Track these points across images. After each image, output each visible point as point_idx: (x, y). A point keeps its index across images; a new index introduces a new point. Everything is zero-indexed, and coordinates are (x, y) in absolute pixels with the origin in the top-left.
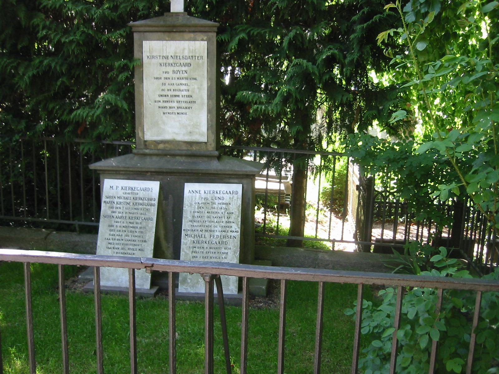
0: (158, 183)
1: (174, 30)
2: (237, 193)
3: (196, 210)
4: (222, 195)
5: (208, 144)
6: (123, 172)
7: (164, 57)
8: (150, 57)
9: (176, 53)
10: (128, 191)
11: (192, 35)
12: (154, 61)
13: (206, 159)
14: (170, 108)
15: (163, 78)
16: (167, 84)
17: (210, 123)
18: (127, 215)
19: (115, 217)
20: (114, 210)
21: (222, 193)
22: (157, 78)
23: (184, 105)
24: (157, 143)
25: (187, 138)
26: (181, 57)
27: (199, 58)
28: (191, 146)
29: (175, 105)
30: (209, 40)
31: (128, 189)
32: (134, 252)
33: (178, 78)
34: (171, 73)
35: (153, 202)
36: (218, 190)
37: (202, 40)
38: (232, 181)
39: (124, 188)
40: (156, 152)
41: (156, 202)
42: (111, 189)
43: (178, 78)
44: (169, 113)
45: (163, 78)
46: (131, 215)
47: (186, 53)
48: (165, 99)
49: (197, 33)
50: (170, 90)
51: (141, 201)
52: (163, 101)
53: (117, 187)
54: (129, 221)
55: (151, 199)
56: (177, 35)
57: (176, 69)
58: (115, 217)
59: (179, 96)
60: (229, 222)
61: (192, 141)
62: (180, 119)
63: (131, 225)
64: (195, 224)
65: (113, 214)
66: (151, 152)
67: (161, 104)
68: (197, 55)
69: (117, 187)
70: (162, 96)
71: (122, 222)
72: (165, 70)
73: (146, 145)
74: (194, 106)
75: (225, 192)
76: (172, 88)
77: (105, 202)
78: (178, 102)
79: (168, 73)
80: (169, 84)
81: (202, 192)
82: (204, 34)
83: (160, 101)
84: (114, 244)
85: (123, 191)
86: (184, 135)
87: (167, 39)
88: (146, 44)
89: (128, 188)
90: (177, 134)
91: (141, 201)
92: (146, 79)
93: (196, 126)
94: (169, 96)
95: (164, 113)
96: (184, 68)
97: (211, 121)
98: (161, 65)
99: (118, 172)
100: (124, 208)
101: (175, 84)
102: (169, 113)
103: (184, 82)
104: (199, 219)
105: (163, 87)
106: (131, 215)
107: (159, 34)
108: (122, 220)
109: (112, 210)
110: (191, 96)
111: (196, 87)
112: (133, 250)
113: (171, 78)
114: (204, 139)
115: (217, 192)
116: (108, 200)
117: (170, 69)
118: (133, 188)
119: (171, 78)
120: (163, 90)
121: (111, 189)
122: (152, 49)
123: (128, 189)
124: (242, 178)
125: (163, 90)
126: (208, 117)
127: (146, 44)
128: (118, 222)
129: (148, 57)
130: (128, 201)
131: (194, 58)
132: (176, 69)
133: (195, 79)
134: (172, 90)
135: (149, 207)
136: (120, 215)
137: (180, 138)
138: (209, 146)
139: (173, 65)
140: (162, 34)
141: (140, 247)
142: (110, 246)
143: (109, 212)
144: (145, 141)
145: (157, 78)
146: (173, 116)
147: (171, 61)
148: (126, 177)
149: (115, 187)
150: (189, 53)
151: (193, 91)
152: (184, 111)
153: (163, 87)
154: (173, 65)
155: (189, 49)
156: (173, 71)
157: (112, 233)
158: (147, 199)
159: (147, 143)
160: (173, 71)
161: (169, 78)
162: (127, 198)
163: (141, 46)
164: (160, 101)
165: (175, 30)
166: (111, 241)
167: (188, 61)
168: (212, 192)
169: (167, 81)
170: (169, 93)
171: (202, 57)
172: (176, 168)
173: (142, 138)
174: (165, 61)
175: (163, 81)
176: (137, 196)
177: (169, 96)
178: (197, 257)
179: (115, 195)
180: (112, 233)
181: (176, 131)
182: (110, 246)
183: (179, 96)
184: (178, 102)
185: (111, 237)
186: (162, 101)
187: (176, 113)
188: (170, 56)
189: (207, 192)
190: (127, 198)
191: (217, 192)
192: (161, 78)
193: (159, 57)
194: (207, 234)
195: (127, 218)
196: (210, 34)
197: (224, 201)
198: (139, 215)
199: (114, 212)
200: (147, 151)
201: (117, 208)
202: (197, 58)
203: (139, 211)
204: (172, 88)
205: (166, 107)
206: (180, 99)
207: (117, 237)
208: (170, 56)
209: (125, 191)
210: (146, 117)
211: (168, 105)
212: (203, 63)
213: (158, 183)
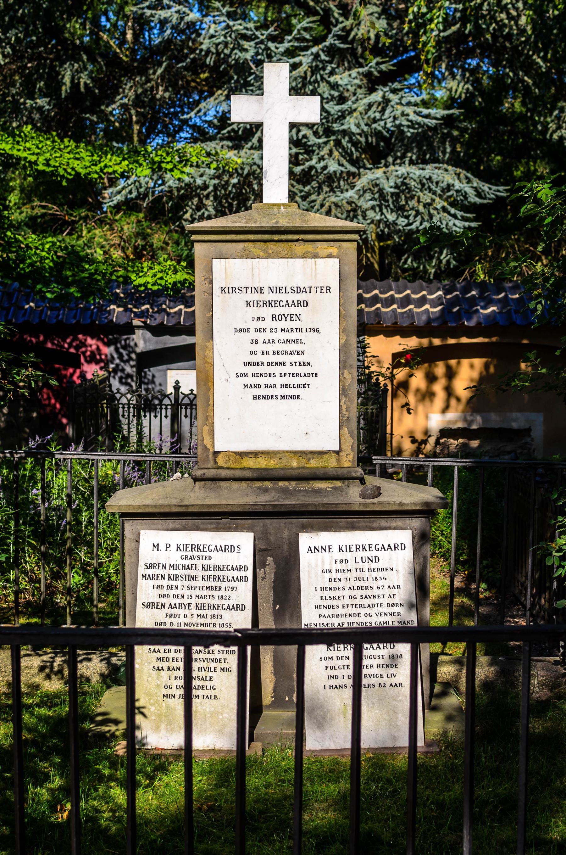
2: (403, 547)
4: (374, 553)
5: (341, 454)
7: (254, 290)
8: (226, 290)
10: (189, 554)
14: (266, 386)
15: (252, 330)
16: (261, 341)
18: (194, 601)
19: (167, 606)
20: (165, 591)
21: (373, 548)
22: (240, 330)
26: (288, 290)
28: (309, 460)
32: (210, 674)
33: (283, 330)
34: (269, 318)
35: (243, 574)
36: (367, 543)
39: (181, 547)
40: (238, 474)
41: (249, 574)
42: (156, 549)
43: (283, 330)
44: (264, 397)
45: (252, 330)
46: (201, 601)
50: (267, 353)
51: (217, 573)
52: (253, 375)
54: (196, 612)
55: (239, 569)
57: (278, 311)
58: (167, 606)
59: (284, 363)
60: (393, 605)
65: (163, 600)
67: (250, 380)
69: (167, 546)
70: (250, 364)
71: (182, 616)
75: (380, 547)
76: (270, 348)
77: (144, 576)
79: (263, 319)
80: (264, 342)
81: (335, 549)
83: (246, 375)
91: (217, 573)
94: (265, 364)
95: (255, 398)
98: (248, 304)
100: (186, 588)
101: (276, 341)
102: (264, 397)
105: (254, 347)
106: (201, 601)
108: (182, 612)
109: (160, 591)
110: (309, 364)
112: (209, 669)
113: (268, 330)
115: (364, 548)
116: (150, 572)
117: (267, 312)
118: (201, 548)
119: (268, 330)
120: (252, 353)
121: (156, 549)
125: (252, 353)
126: (342, 403)
128: (175, 616)
129: (223, 290)
130: (193, 573)
132: (278, 311)
133: (317, 331)
134: (271, 353)
136: (177, 601)
139: (273, 303)
141: (223, 665)
142: (160, 664)
144: (216, 454)
145: (240, 330)
147: (268, 297)
149: (162, 547)
153: (254, 347)
154: (273, 303)
156: (274, 317)
158: (230, 568)
160: (274, 317)
161: (265, 330)
162: (189, 568)
164: (246, 375)
168: (354, 548)
169: (261, 336)
170: (265, 359)
171: (329, 289)
172: (281, 504)
173: (209, 446)
174: (256, 297)
175: (253, 335)
177: (265, 364)
178: (336, 677)
179: (162, 562)
182: (160, 664)
183: (284, 363)
186: (250, 375)
187: (279, 397)
190: (189, 568)
191: (364, 548)
192: (248, 330)
193: (244, 290)
195: (193, 606)
197: (380, 565)
198: (216, 601)
199: (164, 596)
202: (319, 290)
203: (216, 593)
204: (270, 348)
205: (259, 386)
209: (185, 553)
211: (262, 381)
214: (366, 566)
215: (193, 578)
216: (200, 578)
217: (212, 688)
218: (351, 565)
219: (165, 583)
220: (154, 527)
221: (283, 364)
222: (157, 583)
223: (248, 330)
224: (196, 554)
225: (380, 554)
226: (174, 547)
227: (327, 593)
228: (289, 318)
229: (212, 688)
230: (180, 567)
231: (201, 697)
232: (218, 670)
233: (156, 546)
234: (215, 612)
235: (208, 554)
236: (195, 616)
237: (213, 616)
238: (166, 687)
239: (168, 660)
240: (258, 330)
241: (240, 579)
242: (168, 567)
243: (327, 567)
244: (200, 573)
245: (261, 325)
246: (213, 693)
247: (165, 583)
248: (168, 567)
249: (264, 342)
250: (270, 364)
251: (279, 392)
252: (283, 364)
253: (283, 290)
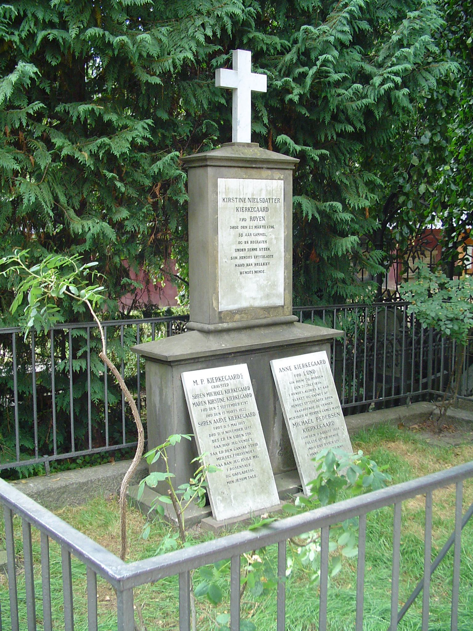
0: (246, 364)
1: (248, 166)
3: (294, 391)
5: (285, 307)
6: (203, 359)
9: (253, 194)
10: (216, 384)
11: (269, 172)
12: (231, 205)
13: (285, 327)
17: (287, 280)
19: (213, 422)
20: (209, 412)
22: (233, 228)
23: (261, 261)
24: (232, 313)
25: (265, 303)
26: (259, 200)
27: (276, 201)
29: (252, 261)
30: (285, 180)
31: (215, 381)
35: (248, 392)
37: (279, 179)
38: (314, 349)
39: (210, 380)
41: (251, 391)
44: (246, 273)
45: (240, 228)
46: (232, 414)
47: (264, 196)
48: (242, 254)
49: (274, 170)
51: (235, 394)
53: (202, 381)
56: (254, 172)
57: (254, 214)
58: (213, 422)
61: (270, 305)
62: (258, 279)
63: (235, 428)
64: (298, 408)
66: (231, 325)
68: (274, 198)
69: (202, 381)
70: (238, 250)
72: (242, 217)
73: (220, 318)
74: (272, 261)
78: (256, 257)
80: (246, 235)
82: (281, 171)
84: (223, 458)
85: (210, 385)
86: (261, 299)
87: (244, 176)
88: (221, 182)
89: (214, 379)
90: (254, 299)
91: (235, 394)
92: (221, 229)
93: (274, 285)
95: (241, 273)
96: (261, 214)
97: (288, 278)
99: (197, 360)
100: (220, 408)
102: (246, 273)
103: (261, 231)
104: (300, 402)
107: (236, 169)
108: (222, 424)
109: (205, 412)
111: (273, 236)
113: (248, 227)
114: (280, 302)
116: (196, 400)
117: (247, 215)
118: (221, 379)
119: (248, 227)
120: (240, 243)
122: (228, 189)
123: (215, 381)
124: (322, 344)
125: (240, 243)
127: (221, 182)
130: (220, 397)
131: (271, 201)
132: (254, 214)
133: (273, 227)
135: (246, 399)
136: (217, 417)
137: (258, 303)
138: (286, 310)
140: (239, 169)
142: (220, 462)
143: (204, 418)
144: (220, 313)
145: (233, 228)
146: (250, 275)
148: (204, 366)
149: (199, 382)
150: (266, 195)
151: (271, 243)
152: (261, 268)
155: (267, 190)
157: (216, 444)
159: (222, 315)
163: (216, 185)
164: (236, 258)
165: (254, 166)
166: (220, 455)
167: (265, 205)
169: (245, 231)
173: (216, 309)
174: (241, 205)
176: (229, 387)
177: (247, 250)
180: (216, 444)
181: (253, 294)
184: (256, 257)
185: (217, 450)
188: (247, 199)
189: (297, 367)
192: (237, 227)
194: (313, 417)
195: (227, 419)
196: (286, 171)
198: (239, 413)
200: (225, 325)
201: (211, 409)
203: (238, 408)
205: (242, 265)
206: (258, 253)
207: (225, 448)
208: (247, 199)
209: (213, 384)
210: (221, 280)
212: (280, 207)
213: (246, 364)
214: (308, 376)
215: (222, 400)
216: (225, 399)
217: (252, 470)
218: (302, 377)
219: (208, 406)
220: (195, 368)
221: (256, 249)
222: (203, 407)
223: (237, 227)
224: (219, 383)
225: (315, 368)
226: (206, 381)
227: (296, 397)
228: (259, 219)
229: (252, 470)
230: (213, 394)
231: (247, 478)
232: (252, 458)
233: (195, 382)
234: (240, 420)
235: (226, 382)
236: (230, 425)
237: (240, 423)
238: (227, 476)
239: (223, 458)
240: (243, 227)
241: (247, 396)
242: (206, 395)
243: (291, 381)
244: (225, 396)
245: (244, 224)
246: (252, 474)
247: (208, 406)
248: (206, 395)
249: (246, 235)
250: (249, 250)
251: (253, 268)
252: (256, 249)
253: (256, 201)
